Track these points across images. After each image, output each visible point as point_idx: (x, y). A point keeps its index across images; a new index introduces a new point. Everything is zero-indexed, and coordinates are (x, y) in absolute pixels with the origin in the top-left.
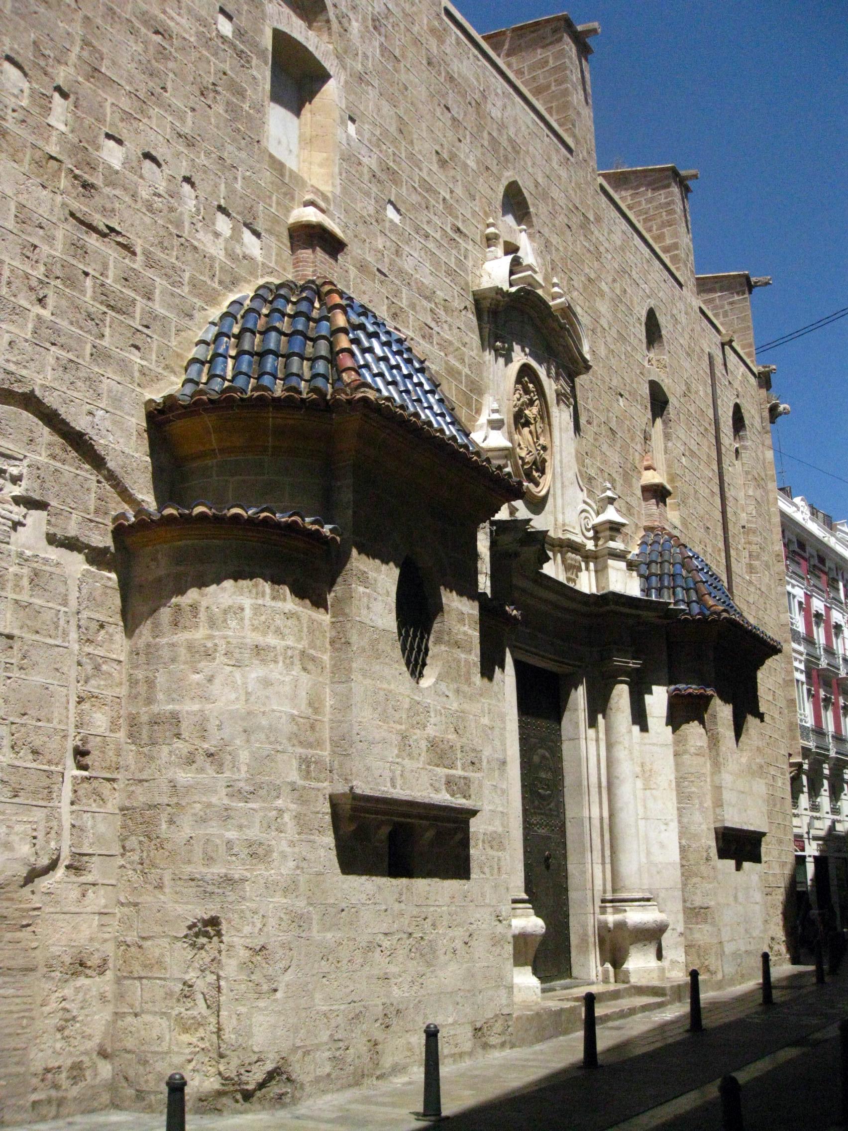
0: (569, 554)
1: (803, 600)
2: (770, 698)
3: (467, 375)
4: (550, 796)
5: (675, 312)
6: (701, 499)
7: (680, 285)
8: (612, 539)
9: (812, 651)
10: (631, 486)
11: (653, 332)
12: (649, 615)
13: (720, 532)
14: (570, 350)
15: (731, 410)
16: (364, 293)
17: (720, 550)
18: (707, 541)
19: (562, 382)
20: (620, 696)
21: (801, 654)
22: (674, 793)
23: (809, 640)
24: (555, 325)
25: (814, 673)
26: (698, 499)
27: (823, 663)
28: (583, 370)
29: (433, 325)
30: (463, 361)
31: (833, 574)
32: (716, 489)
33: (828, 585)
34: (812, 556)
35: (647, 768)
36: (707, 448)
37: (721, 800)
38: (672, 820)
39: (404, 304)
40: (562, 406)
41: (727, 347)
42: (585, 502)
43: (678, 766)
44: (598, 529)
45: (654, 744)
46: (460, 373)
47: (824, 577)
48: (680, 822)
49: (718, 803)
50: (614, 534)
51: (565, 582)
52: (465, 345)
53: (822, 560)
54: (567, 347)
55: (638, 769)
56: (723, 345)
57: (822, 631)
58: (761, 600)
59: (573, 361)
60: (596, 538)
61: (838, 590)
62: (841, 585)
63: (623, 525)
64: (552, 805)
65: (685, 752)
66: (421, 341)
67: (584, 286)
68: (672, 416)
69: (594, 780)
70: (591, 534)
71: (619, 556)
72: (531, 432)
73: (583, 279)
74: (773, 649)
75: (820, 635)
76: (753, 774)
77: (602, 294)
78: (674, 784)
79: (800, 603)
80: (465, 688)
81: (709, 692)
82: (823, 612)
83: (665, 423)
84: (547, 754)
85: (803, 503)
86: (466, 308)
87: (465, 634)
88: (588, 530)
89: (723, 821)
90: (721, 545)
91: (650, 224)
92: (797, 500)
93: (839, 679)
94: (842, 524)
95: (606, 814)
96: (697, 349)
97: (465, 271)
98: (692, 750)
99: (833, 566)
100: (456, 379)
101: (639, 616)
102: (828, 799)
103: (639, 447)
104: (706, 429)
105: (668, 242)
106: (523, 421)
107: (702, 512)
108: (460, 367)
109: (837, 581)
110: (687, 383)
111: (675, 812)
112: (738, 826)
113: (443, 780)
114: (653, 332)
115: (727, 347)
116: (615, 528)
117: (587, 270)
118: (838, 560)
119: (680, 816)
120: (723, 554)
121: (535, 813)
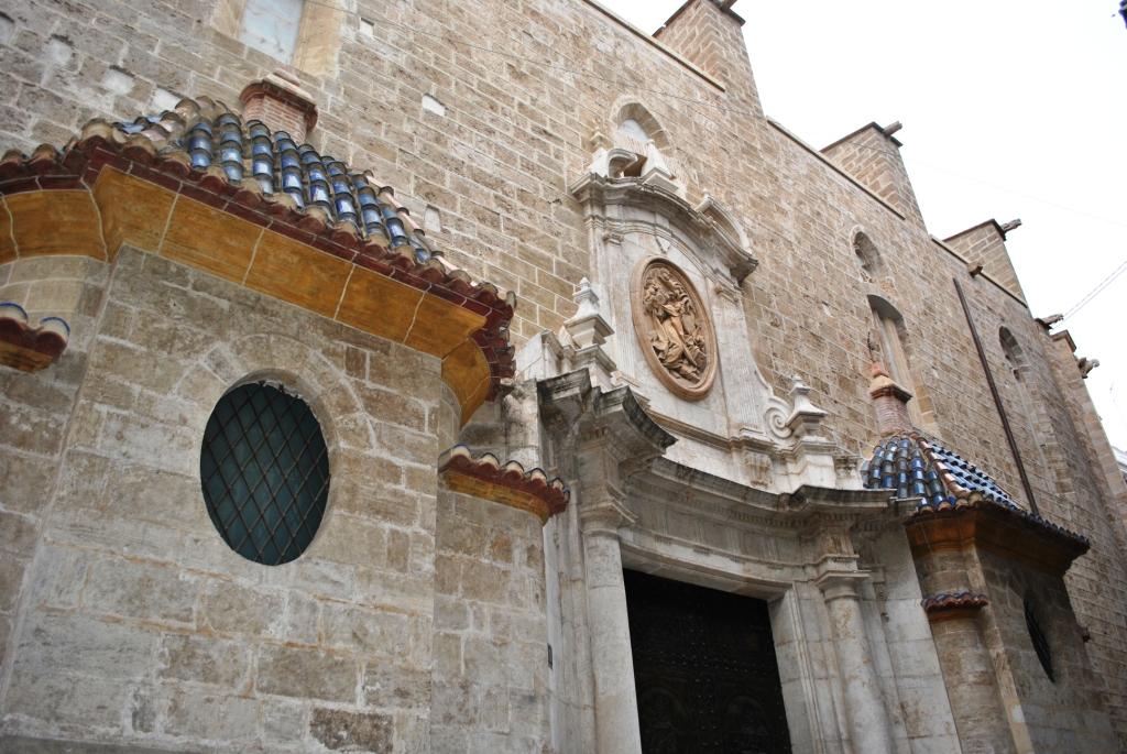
3: (558, 263)
5: (896, 239)
6: (969, 412)
7: (903, 219)
10: (853, 392)
15: (997, 336)
17: (1008, 465)
18: (987, 454)
26: (965, 413)
29: (499, 210)
30: (553, 249)
32: (991, 404)
35: (909, 710)
36: (969, 362)
39: (448, 186)
42: (771, 400)
46: (549, 260)
52: (557, 234)
63: (822, 416)
66: (477, 223)
72: (673, 325)
73: (751, 195)
77: (784, 213)
80: (393, 574)
86: (558, 201)
87: (395, 493)
96: (936, 275)
97: (559, 169)
100: (539, 265)
103: (861, 355)
104: (963, 348)
107: (973, 425)
108: (548, 254)
110: (925, 304)
113: (309, 717)
120: (1015, 470)
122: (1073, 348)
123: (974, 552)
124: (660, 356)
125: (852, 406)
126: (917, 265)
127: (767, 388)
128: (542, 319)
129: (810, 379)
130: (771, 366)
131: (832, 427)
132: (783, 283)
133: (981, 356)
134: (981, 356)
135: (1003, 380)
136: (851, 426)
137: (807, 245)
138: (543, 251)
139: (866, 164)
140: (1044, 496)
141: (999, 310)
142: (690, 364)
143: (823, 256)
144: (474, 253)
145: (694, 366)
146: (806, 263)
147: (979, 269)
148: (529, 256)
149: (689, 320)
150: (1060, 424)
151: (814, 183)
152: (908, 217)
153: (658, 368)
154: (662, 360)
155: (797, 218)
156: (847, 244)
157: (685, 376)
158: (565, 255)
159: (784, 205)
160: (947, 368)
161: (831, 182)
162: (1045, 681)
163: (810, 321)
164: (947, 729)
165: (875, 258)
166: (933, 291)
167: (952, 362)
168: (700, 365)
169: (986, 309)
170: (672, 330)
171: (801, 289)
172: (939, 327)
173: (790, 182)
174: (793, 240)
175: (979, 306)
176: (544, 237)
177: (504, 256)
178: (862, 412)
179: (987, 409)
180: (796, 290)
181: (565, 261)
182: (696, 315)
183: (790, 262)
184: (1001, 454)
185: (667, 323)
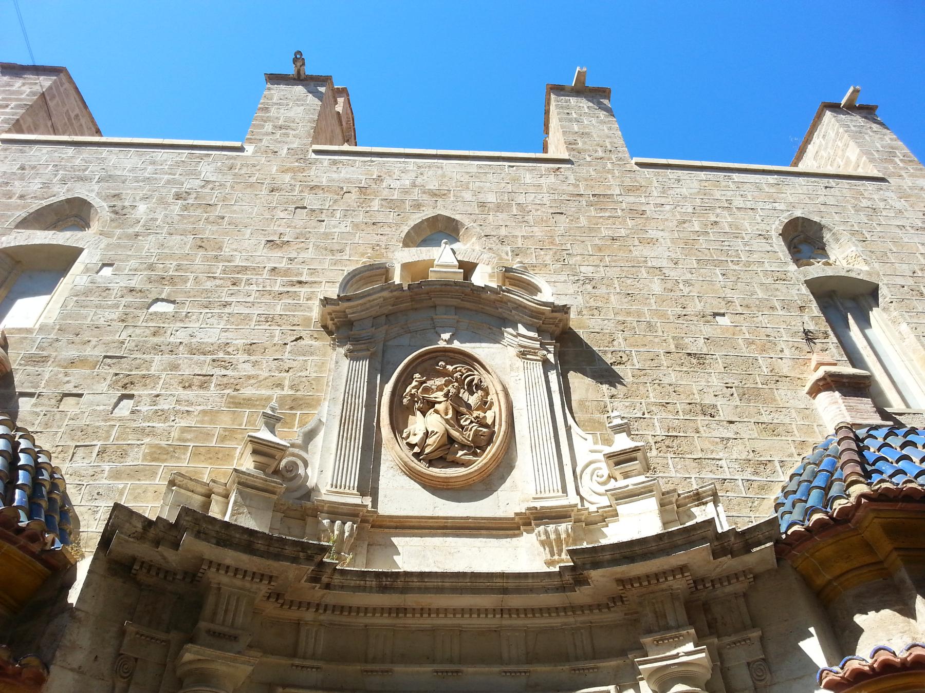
14: (525, 307)
16: (68, 382)
72: (437, 412)
77: (652, 242)
101: (682, 569)
117: (604, 232)
125: (765, 418)
132: (639, 314)
136: (759, 445)
138: (263, 392)
143: (718, 263)
144: (166, 420)
148: (248, 402)
152: (893, 175)
153: (406, 464)
154: (416, 455)
158: (291, 387)
159: (652, 234)
173: (668, 208)
174: (664, 263)
177: (204, 412)
178: (787, 421)
180: (663, 315)
183: (657, 287)
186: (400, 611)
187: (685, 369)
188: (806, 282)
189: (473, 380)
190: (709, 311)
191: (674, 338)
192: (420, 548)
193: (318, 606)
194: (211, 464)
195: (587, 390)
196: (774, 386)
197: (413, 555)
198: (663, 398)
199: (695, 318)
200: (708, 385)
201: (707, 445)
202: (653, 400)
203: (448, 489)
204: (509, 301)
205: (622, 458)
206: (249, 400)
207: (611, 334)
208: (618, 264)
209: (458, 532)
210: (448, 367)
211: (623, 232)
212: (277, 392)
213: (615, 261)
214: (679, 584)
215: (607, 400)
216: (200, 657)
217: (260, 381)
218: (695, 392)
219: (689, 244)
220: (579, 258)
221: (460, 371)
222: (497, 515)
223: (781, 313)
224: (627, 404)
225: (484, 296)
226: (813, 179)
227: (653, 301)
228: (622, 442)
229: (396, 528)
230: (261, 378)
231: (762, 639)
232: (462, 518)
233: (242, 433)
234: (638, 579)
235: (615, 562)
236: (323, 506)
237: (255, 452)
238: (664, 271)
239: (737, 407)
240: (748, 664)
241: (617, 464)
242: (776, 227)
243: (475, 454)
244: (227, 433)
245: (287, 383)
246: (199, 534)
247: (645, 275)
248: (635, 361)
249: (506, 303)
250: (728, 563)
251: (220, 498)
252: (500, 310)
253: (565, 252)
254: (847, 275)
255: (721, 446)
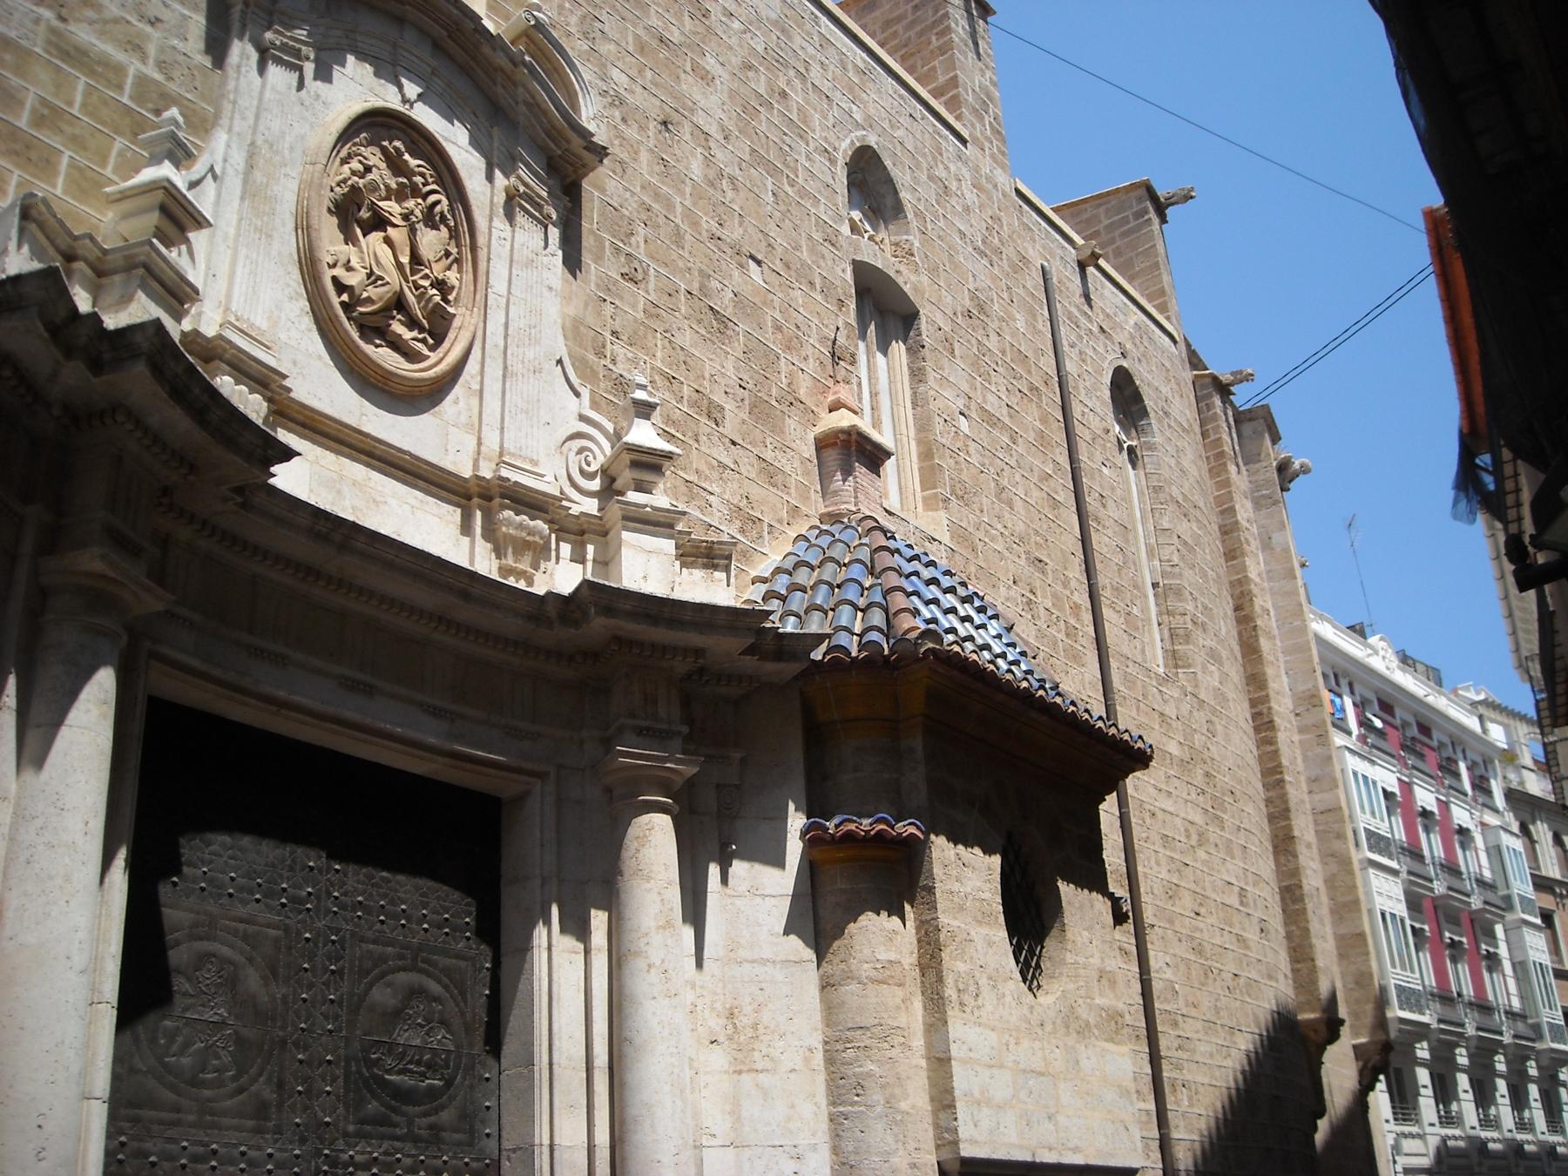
0: (508, 514)
1: (1396, 790)
2: (1234, 900)
4: (432, 1093)
5: (940, 172)
6: (1018, 504)
7: (964, 141)
8: (641, 487)
9: (1417, 867)
10: (778, 430)
11: (870, 184)
12: (724, 646)
13: (1076, 572)
14: (545, 112)
15: (1107, 379)
17: (1076, 608)
18: (1038, 584)
19: (523, 172)
20: (643, 840)
21: (1395, 873)
22: (821, 1078)
23: (1414, 853)
24: (501, 60)
25: (1427, 905)
26: (1010, 504)
27: (1439, 888)
28: (588, 157)
31: (1449, 752)
33: (1441, 767)
34: (1405, 724)
35: (744, 1021)
36: (1039, 416)
37: (949, 1091)
38: (814, 1147)
40: (520, 218)
41: (1091, 270)
43: (830, 1010)
44: (613, 472)
45: (764, 962)
47: (1432, 757)
48: (835, 1150)
49: (943, 1100)
50: (647, 476)
51: (495, 576)
53: (1425, 730)
54: (535, 106)
55: (716, 1023)
56: (1082, 266)
57: (1436, 839)
58: (1200, 717)
59: (553, 133)
60: (610, 491)
61: (1457, 775)
62: (1462, 767)
63: (669, 456)
64: (446, 1116)
65: (849, 977)
67: (642, 48)
68: (926, 339)
69: (570, 1047)
70: (595, 485)
71: (657, 523)
72: (388, 241)
73: (640, 32)
74: (1142, 759)
75: (1432, 846)
76: (1084, 1031)
77: (706, 78)
78: (819, 1058)
79: (1388, 795)
81: (906, 828)
82: (1436, 811)
83: (915, 351)
84: (434, 987)
85: (1382, 644)
88: (590, 476)
89: (955, 1143)
90: (1083, 599)
91: (911, 62)
92: (1373, 640)
93: (1471, 913)
94: (1467, 689)
95: (602, 1137)
96: (1009, 251)
98: (866, 970)
99: (1446, 740)
101: (698, 652)
102: (1432, 1102)
103: (811, 366)
104: (1033, 388)
105: (942, 79)
106: (365, 214)
107: (1020, 527)
108: (119, 56)
109: (1456, 762)
110: (974, 297)
111: (824, 1125)
112: (1026, 1157)
114: (870, 184)
115: (1091, 270)
116: (649, 464)
117: (654, 21)
118: (1452, 729)
119: (836, 1136)
120: (1087, 617)
121: (360, 1135)
122: (1276, 438)
123: (918, 744)
124: (345, 297)
125: (768, 455)
126: (975, 227)
127: (577, 394)
128: (70, 179)
129: (686, 390)
130: (601, 354)
131: (714, 488)
132: (670, 206)
133: (1065, 409)
134: (1065, 409)
135: (1099, 458)
136: (755, 492)
137: (742, 148)
139: (921, 34)
140: (1132, 669)
141: (1119, 337)
142: (412, 323)
143: (774, 171)
145: (422, 329)
146: (732, 179)
147: (1095, 257)
149: (431, 241)
150: (1191, 550)
151: (790, 38)
152: (976, 141)
155: (733, 94)
156: (833, 161)
157: (396, 345)
158: (161, 65)
159: (710, 63)
160: (990, 419)
161: (826, 42)
162: (1015, 984)
163: (714, 284)
164: (807, 1060)
165: (889, 201)
166: (995, 278)
167: (1005, 410)
168: (437, 327)
169: (1095, 329)
170: (385, 253)
171: (708, 223)
172: (993, 343)
173: (736, 25)
174: (713, 130)
175: (1083, 320)
176: (116, 21)
178: (788, 469)
179: (1055, 504)
180: (695, 224)
181: (158, 76)
182: (454, 234)
183: (696, 169)
184: (1065, 585)
185: (376, 236)
186: (311, 572)
187: (703, 332)
188: (854, 262)
189: (438, 202)
190: (746, 249)
191: (701, 271)
192: (335, 476)
193: (204, 523)
194: (17, 165)
195: (586, 305)
196: (786, 409)
197: (305, 475)
198: (670, 366)
199: (729, 251)
200: (722, 369)
201: (703, 467)
202: (659, 364)
203: (384, 391)
204: (524, 86)
205: (645, 458)
206: (85, 53)
207: (631, 221)
208: (658, 93)
209: (388, 468)
210: (407, 157)
211: (676, 36)
212: (134, 67)
213: (656, 85)
214: (681, 667)
215: (608, 335)
216: (111, 574)
217: (106, 22)
218: (707, 376)
219: (747, 110)
220: (612, 47)
221: (422, 175)
222: (441, 464)
223: (819, 298)
224: (630, 355)
225: (486, 50)
226: (903, 92)
227: (688, 190)
228: (643, 434)
229: (304, 425)
230: (107, 15)
231: (743, 760)
232: (400, 450)
233: (72, 125)
234: (641, 644)
235: (633, 616)
236: (225, 350)
237: (164, 209)
238: (712, 145)
239: (744, 422)
240: (718, 786)
241: (635, 464)
242: (845, 149)
243: (423, 341)
244: (46, 112)
245: (152, 50)
246: (157, 369)
247: (687, 137)
248: (651, 286)
249: (515, 84)
250: (750, 663)
251: (89, 272)
252: (500, 90)
253: (598, 24)
254: (892, 274)
255: (715, 475)
